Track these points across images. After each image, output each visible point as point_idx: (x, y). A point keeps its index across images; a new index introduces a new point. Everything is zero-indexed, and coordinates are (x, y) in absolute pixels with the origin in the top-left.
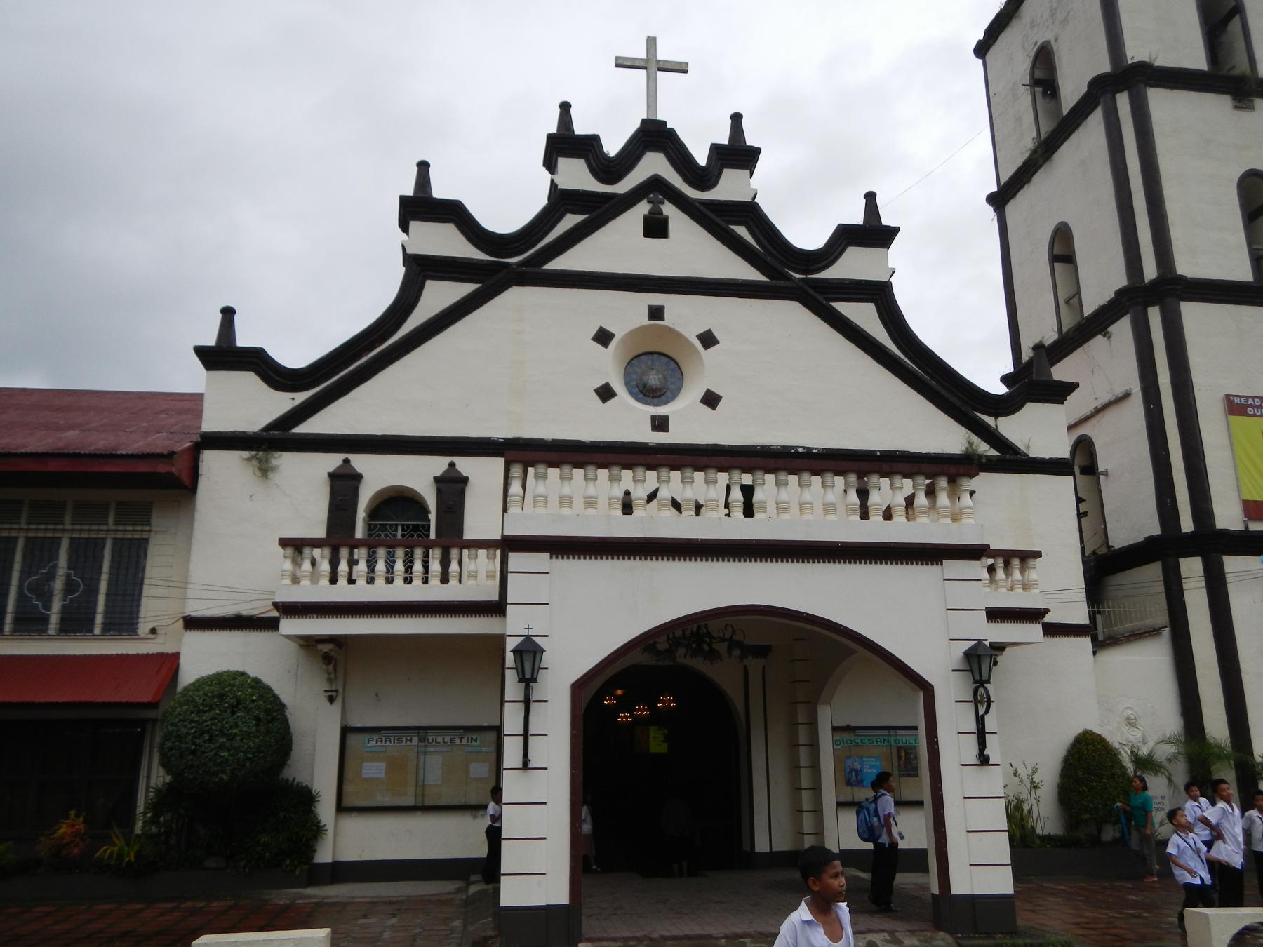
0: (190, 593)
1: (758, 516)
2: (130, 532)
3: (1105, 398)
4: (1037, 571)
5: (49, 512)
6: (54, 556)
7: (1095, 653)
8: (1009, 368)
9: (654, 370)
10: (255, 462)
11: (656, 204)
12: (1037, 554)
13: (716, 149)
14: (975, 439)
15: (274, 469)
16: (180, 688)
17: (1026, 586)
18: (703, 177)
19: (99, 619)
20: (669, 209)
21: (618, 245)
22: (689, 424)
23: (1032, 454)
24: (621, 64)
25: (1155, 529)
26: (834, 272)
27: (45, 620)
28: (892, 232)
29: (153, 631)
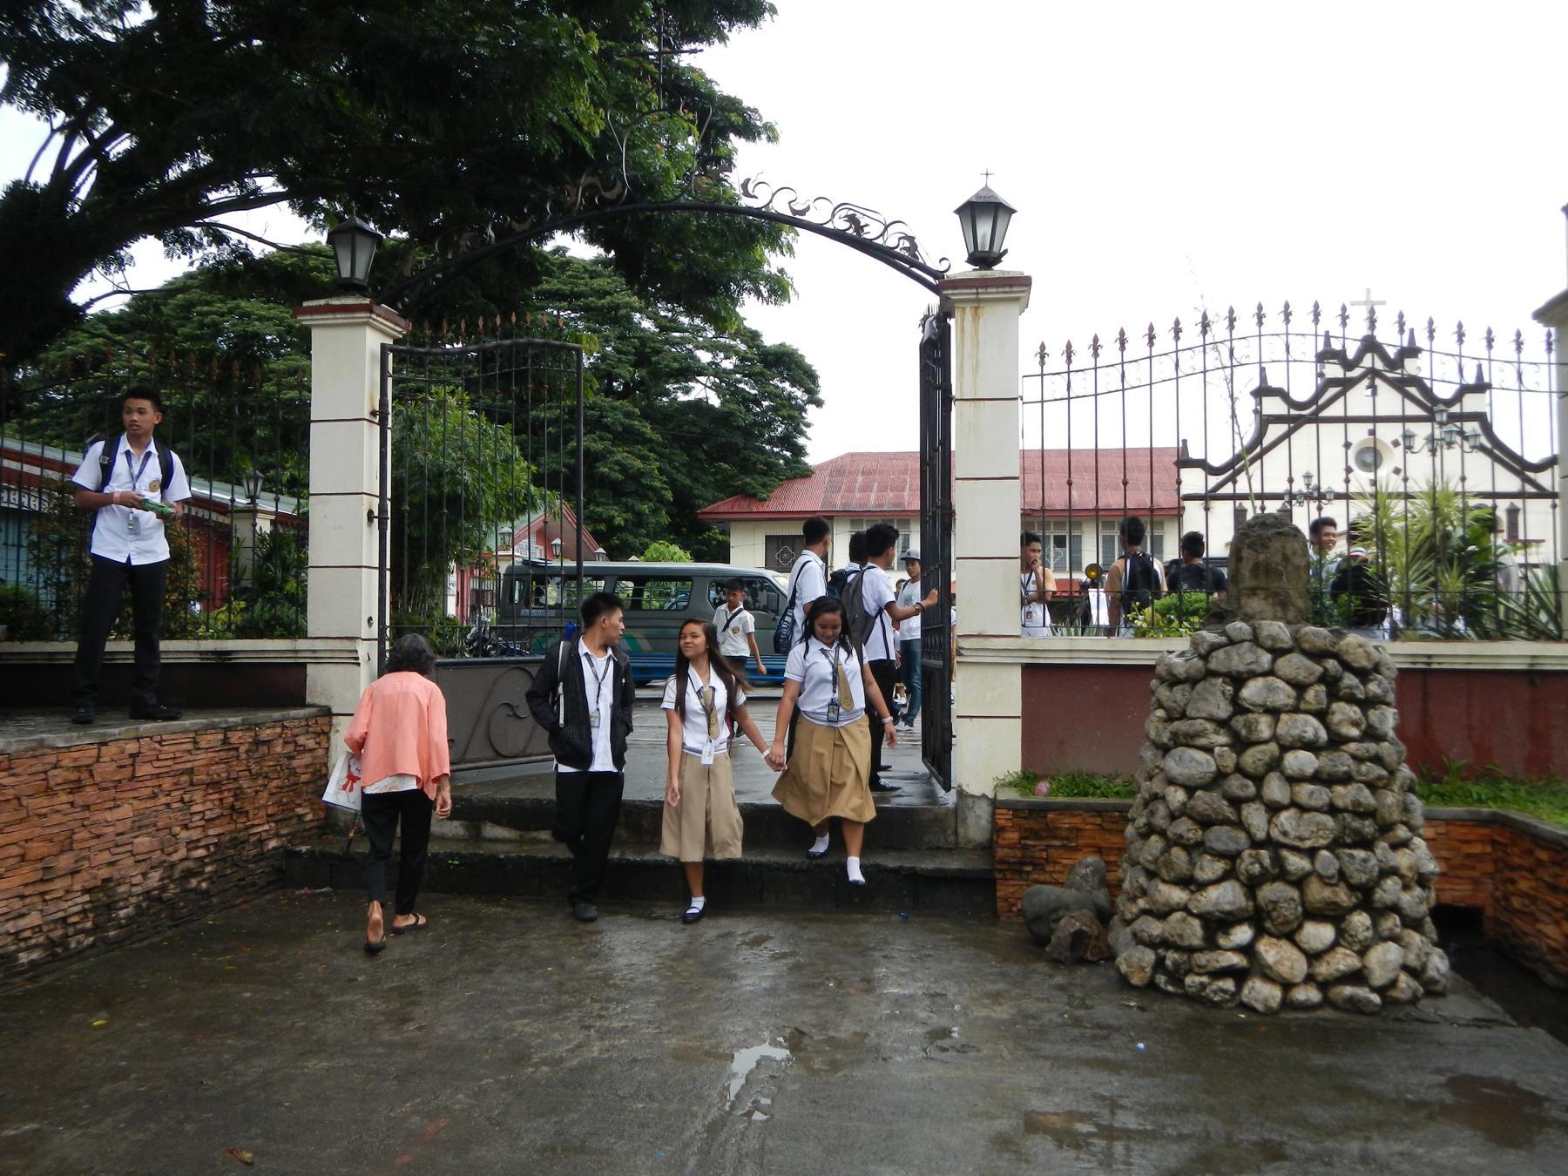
11: (1373, 380)
20: (1378, 382)
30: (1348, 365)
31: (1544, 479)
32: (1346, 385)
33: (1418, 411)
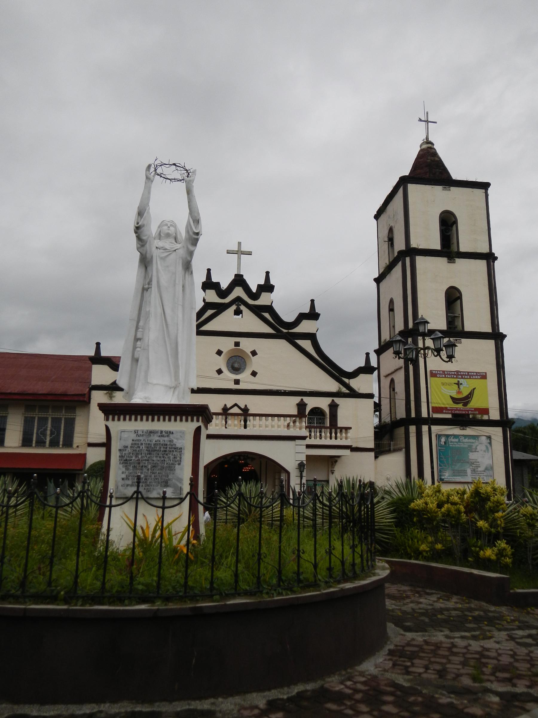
0: (89, 436)
1: (248, 428)
2: (70, 416)
3: (397, 367)
4: (350, 433)
5: (44, 408)
6: (46, 423)
7: (376, 457)
8: (377, 347)
9: (237, 362)
10: (108, 395)
11: (238, 306)
12: (350, 428)
13: (259, 286)
14: (341, 386)
15: (114, 397)
16: (88, 466)
17: (346, 438)
18: (255, 296)
19: (61, 443)
20: (242, 308)
21: (227, 321)
22: (246, 381)
23: (361, 392)
24: (228, 252)
25: (404, 416)
26: (297, 330)
27: (45, 442)
28: (319, 315)
29: (78, 447)
30: (223, 294)
31: (360, 384)
32: (220, 308)
33: (268, 330)
